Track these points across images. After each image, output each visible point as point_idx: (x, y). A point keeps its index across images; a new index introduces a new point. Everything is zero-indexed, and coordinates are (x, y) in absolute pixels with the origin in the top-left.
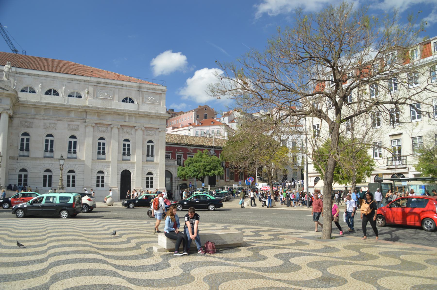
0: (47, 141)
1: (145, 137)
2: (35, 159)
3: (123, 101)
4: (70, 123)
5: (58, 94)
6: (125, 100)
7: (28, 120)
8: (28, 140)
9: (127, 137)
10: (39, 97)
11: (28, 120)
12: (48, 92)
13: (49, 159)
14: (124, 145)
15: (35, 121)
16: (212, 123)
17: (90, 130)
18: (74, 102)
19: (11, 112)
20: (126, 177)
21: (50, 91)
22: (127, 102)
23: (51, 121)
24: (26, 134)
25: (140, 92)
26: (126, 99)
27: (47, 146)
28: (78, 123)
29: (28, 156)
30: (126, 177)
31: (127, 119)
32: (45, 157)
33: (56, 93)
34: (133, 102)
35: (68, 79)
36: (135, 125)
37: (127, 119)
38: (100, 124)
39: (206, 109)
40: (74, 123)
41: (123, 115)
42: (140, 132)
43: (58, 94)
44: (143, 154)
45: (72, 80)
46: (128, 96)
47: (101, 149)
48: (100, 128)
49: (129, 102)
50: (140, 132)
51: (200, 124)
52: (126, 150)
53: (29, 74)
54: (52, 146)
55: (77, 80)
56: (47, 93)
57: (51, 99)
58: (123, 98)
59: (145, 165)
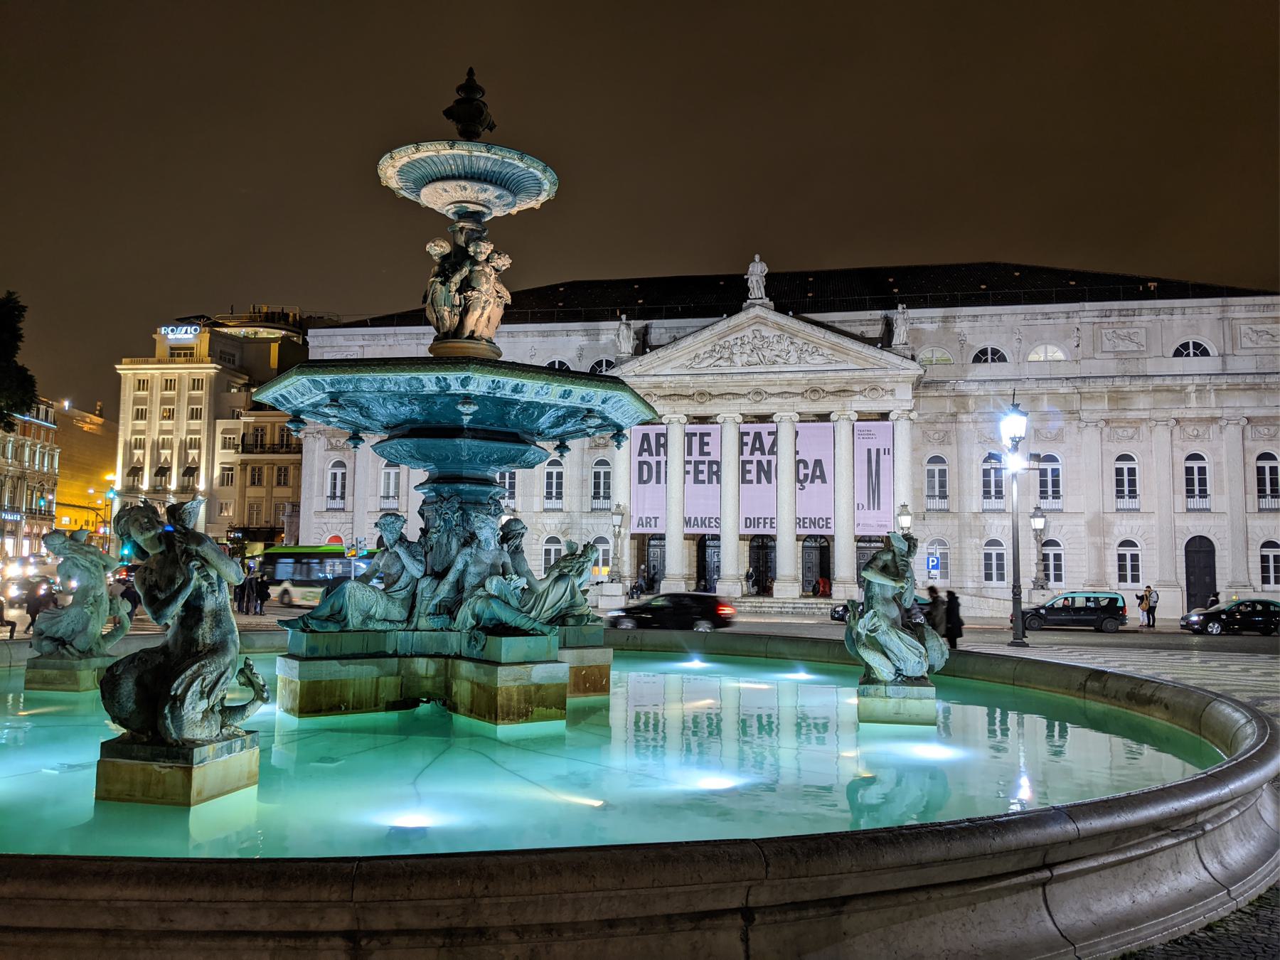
3: (1178, 353)
6: (1181, 352)
14: (1189, 471)
17: (1091, 435)
22: (1188, 355)
25: (1226, 322)
26: (1185, 346)
31: (1193, 403)
34: (1205, 353)
37: (1193, 403)
38: (1118, 420)
41: (1180, 391)
47: (1125, 484)
48: (1120, 431)
49: (1195, 355)
52: (1195, 483)
58: (1177, 345)
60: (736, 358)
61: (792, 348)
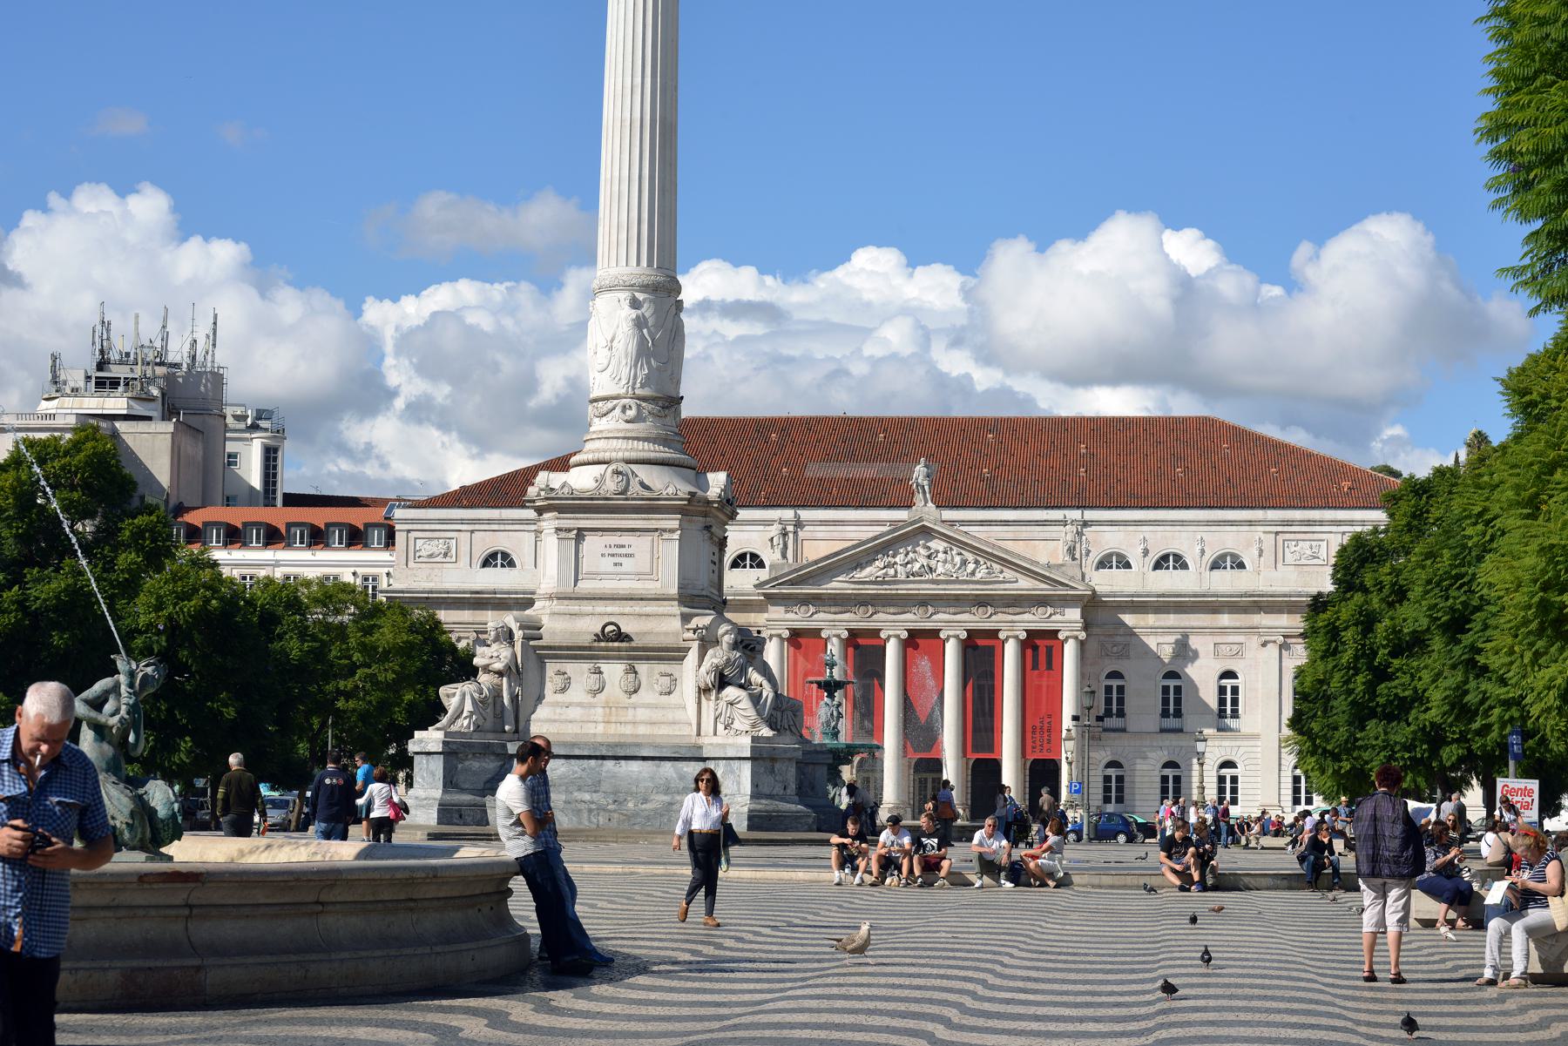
0: (1166, 689)
4: (1219, 639)
5: (1185, 566)
7: (1118, 639)
8: (1121, 689)
10: (1140, 580)
11: (1118, 639)
13: (1172, 736)
18: (1226, 583)
19: (1082, 635)
21: (1165, 558)
24: (1115, 675)
27: (1165, 702)
28: (1240, 639)
29: (1124, 730)
32: (1163, 731)
33: (1180, 563)
35: (1209, 523)
40: (1231, 639)
43: (1185, 566)
53: (1112, 523)
54: (1178, 702)
56: (1157, 566)
60: (899, 568)
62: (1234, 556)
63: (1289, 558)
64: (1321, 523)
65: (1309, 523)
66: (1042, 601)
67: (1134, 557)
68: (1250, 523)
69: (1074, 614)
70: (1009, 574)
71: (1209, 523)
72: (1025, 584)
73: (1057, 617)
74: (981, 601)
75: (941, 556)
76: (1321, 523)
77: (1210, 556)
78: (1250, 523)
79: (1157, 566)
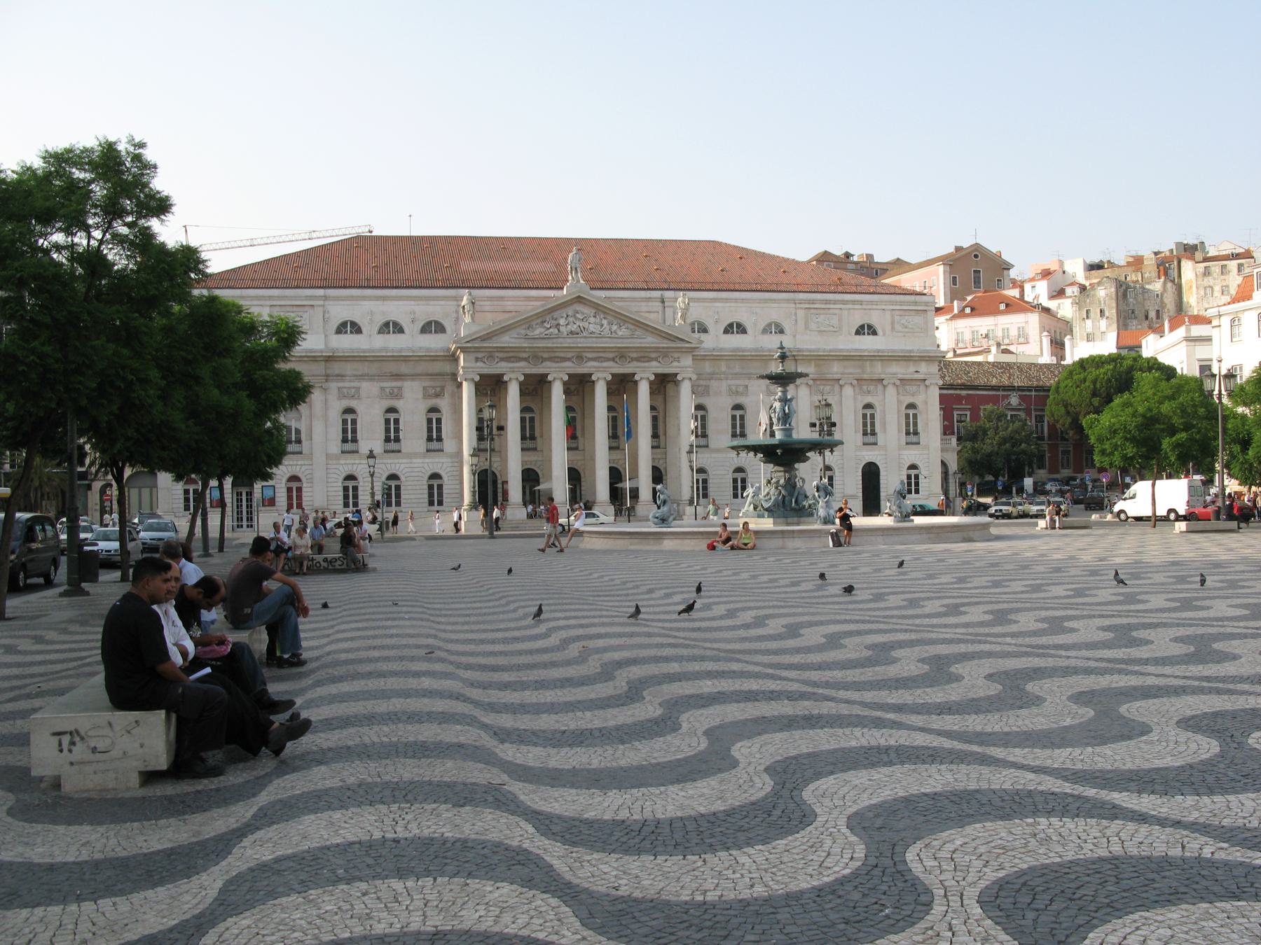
0: (734, 417)
1: (902, 398)
2: (718, 451)
3: (858, 333)
9: (868, 399)
10: (715, 340)
12: (729, 329)
15: (714, 384)
16: (1002, 307)
20: (871, 475)
21: (731, 325)
23: (737, 382)
30: (871, 475)
33: (741, 329)
34: (875, 333)
36: (883, 376)
39: (976, 256)
42: (891, 391)
43: (744, 331)
44: (899, 431)
45: (766, 301)
46: (866, 321)
50: (891, 391)
51: (968, 310)
55: (774, 301)
56: (726, 331)
57: (735, 341)
59: (905, 452)
60: (562, 329)
61: (605, 322)
62: (777, 325)
63: (813, 326)
64: (835, 302)
65: (827, 302)
66: (664, 354)
67: (709, 324)
68: (788, 301)
69: (687, 361)
70: (639, 332)
71: (761, 301)
72: (650, 341)
73: (675, 364)
74: (621, 355)
75: (592, 320)
76: (835, 302)
77: (762, 326)
78: (788, 301)
79: (726, 331)
